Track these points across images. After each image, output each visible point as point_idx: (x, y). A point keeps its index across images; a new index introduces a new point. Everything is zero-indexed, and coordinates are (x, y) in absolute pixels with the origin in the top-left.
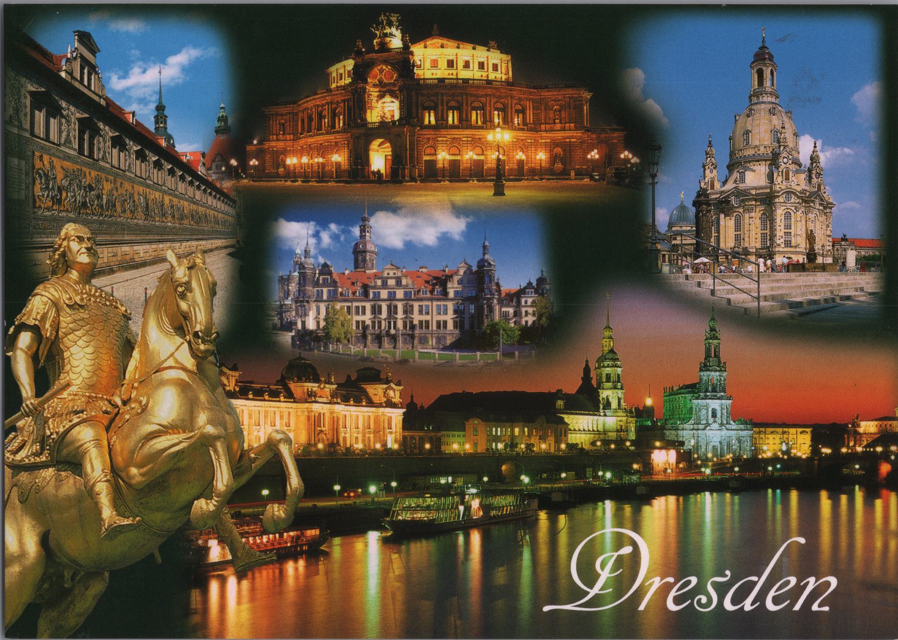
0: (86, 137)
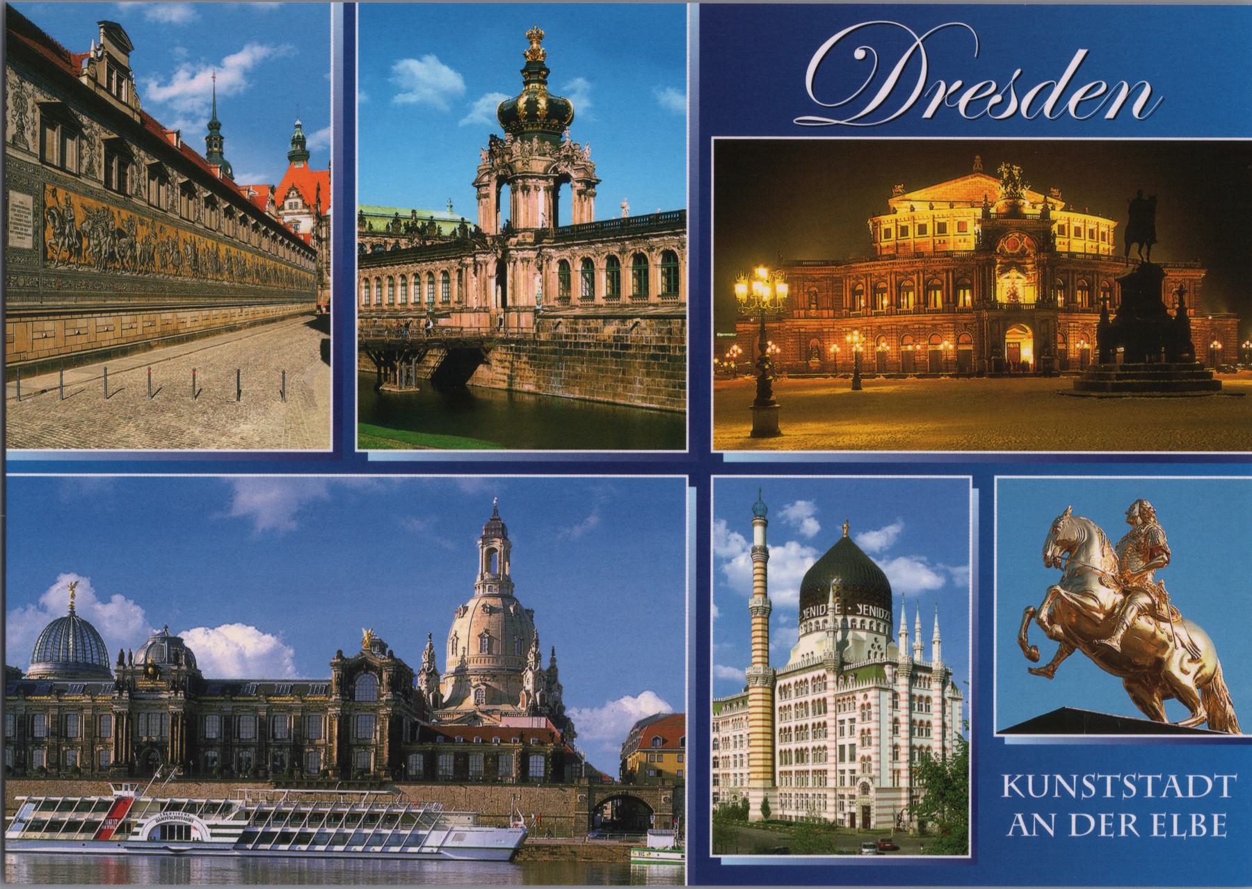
0: (115, 164)
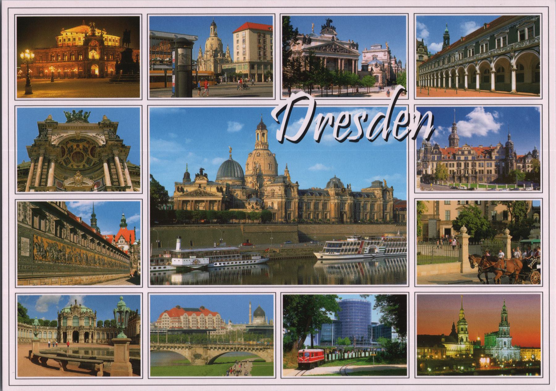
0: (58, 228)
